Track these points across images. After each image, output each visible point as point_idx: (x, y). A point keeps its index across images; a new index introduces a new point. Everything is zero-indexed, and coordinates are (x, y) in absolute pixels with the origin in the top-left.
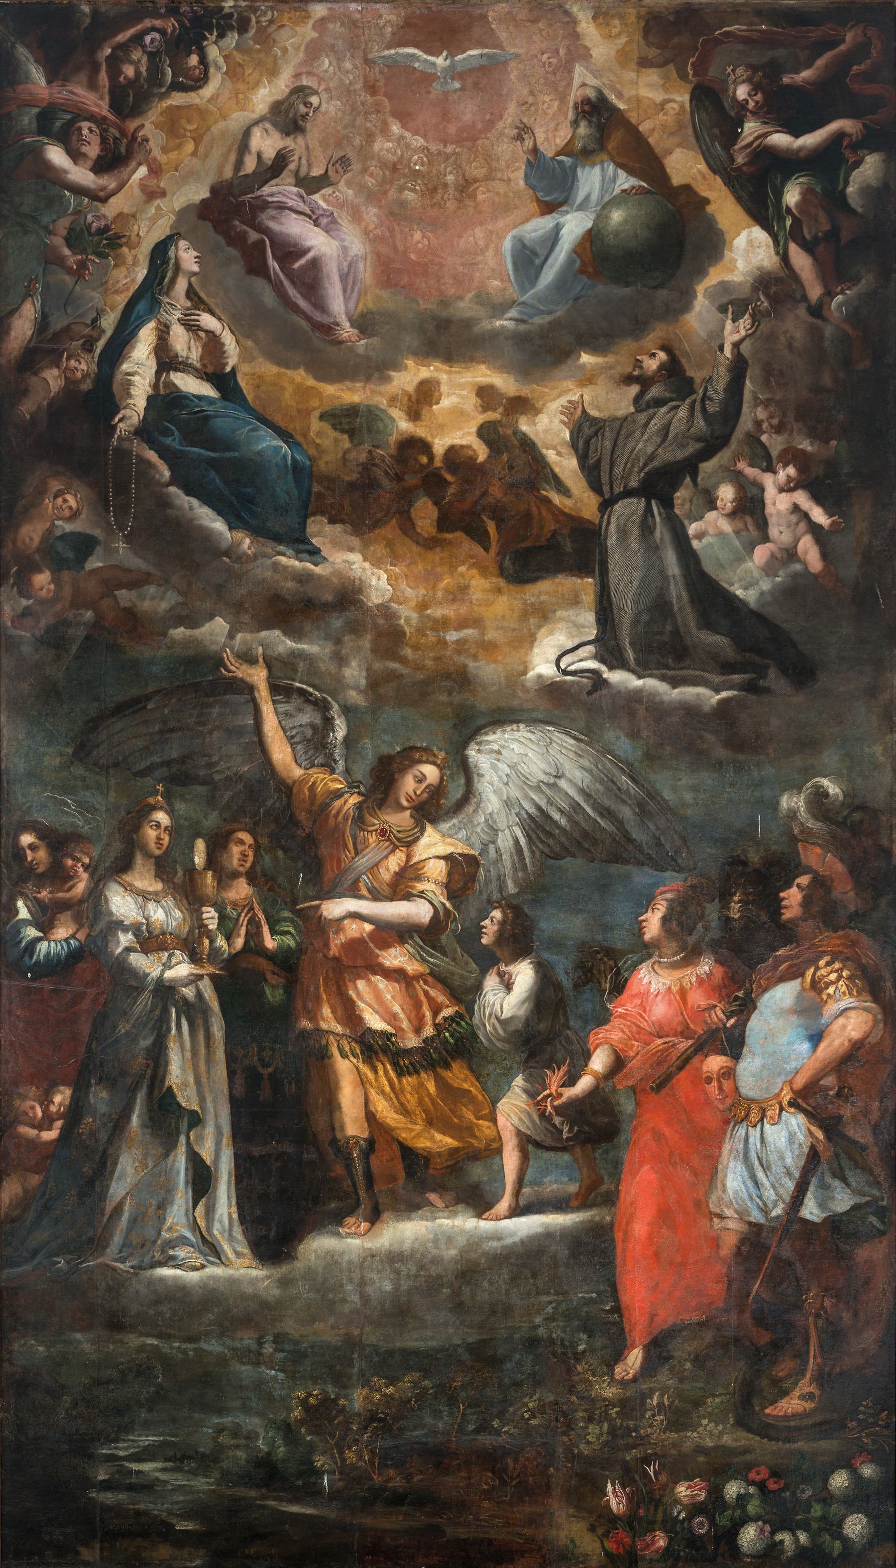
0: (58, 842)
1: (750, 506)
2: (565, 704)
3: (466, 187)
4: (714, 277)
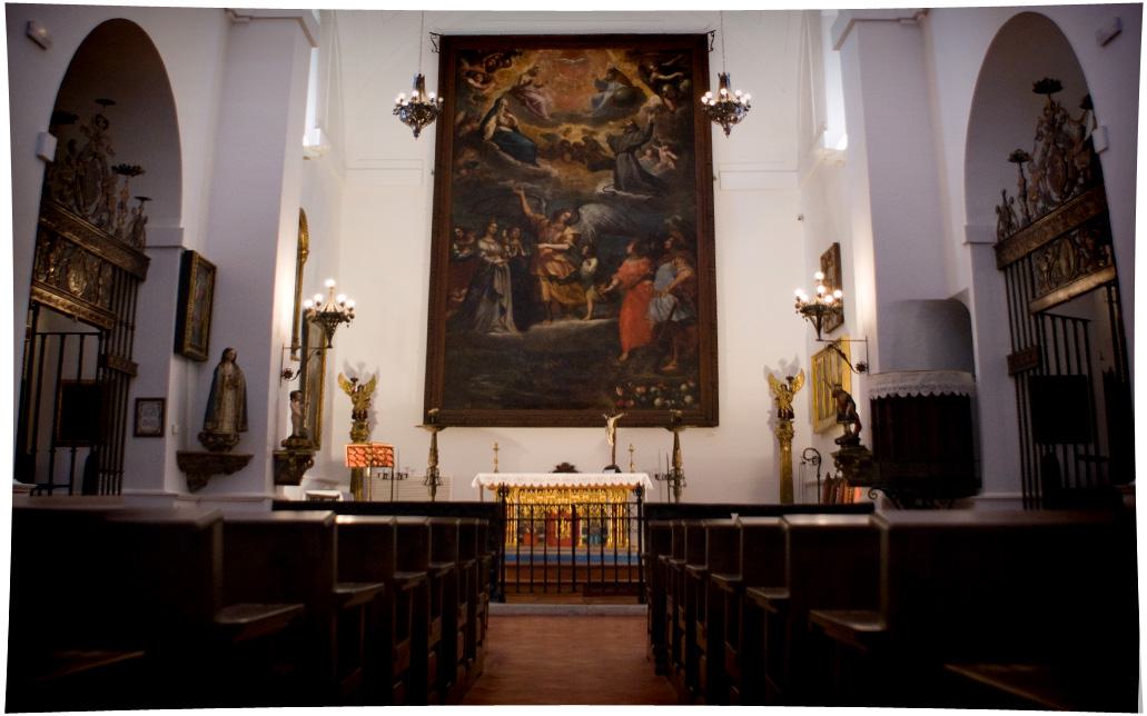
0: (466, 231)
1: (655, 155)
2: (603, 199)
3: (579, 87)
4: (645, 105)
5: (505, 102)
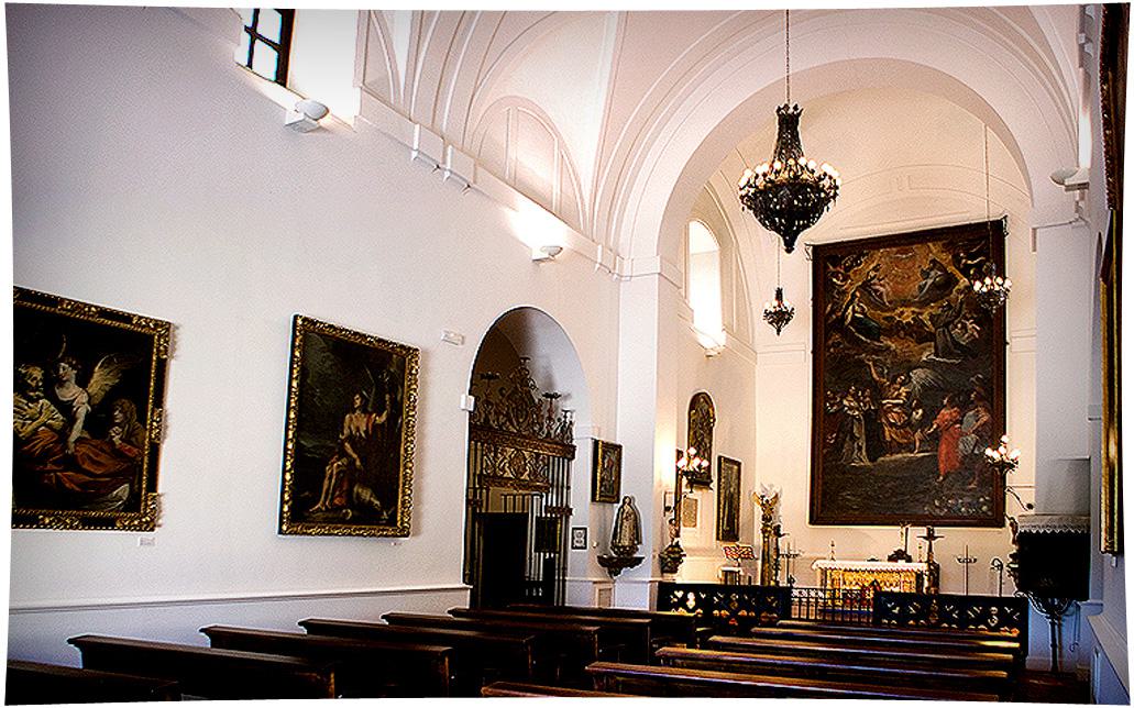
0: (834, 393)
1: (964, 327)
2: (929, 364)
3: (909, 277)
4: (957, 287)
5: (858, 294)
